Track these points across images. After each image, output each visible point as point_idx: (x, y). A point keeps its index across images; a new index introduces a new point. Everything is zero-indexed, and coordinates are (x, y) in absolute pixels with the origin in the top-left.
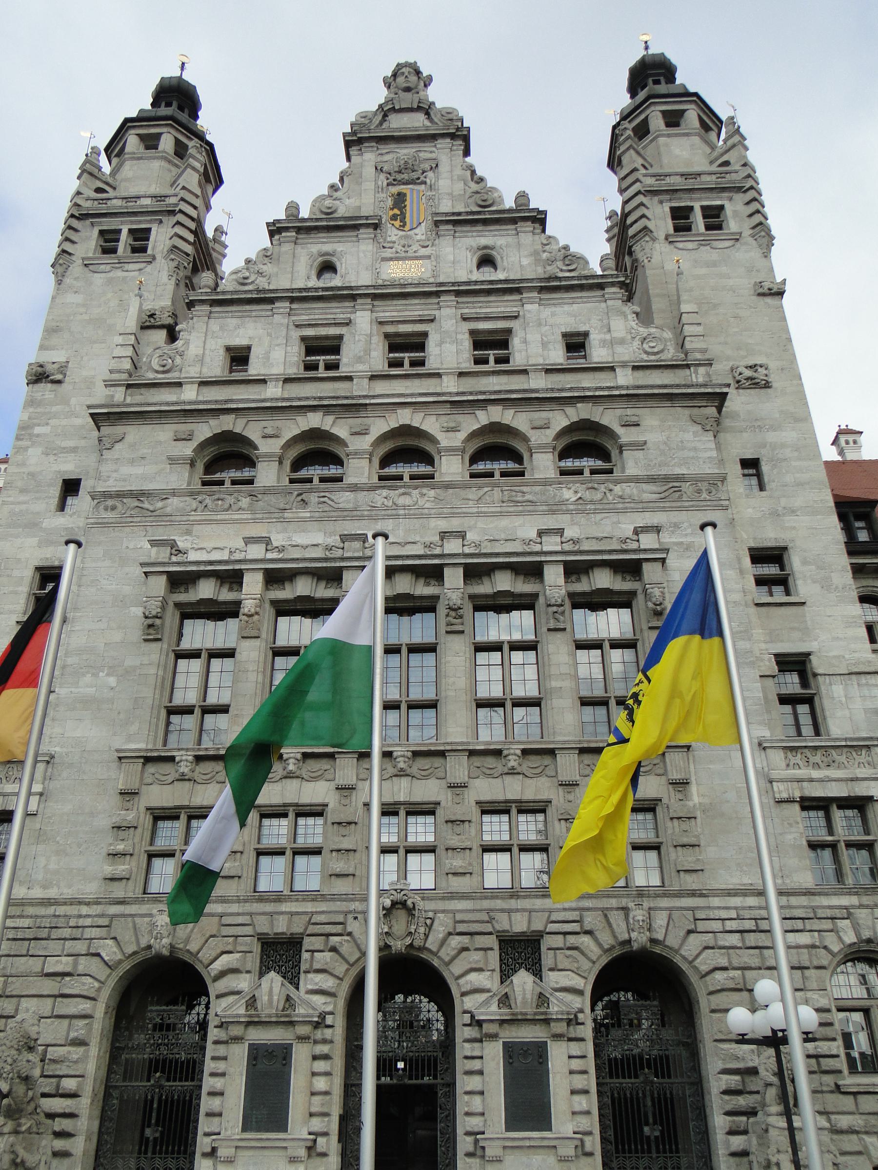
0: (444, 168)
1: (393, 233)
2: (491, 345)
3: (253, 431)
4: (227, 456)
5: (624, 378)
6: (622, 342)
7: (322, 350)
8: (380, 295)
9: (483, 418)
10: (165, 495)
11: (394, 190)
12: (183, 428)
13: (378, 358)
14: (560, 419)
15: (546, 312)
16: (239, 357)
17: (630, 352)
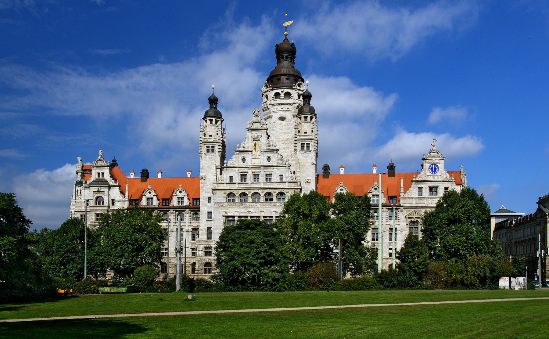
0: (263, 137)
1: (254, 152)
2: (269, 175)
3: (235, 192)
4: (230, 195)
5: (287, 185)
6: (287, 177)
7: (244, 176)
9: (267, 191)
10: (224, 203)
11: (255, 142)
12: (225, 191)
13: (252, 181)
14: (278, 191)
15: (277, 171)
16: (231, 177)
17: (289, 179)
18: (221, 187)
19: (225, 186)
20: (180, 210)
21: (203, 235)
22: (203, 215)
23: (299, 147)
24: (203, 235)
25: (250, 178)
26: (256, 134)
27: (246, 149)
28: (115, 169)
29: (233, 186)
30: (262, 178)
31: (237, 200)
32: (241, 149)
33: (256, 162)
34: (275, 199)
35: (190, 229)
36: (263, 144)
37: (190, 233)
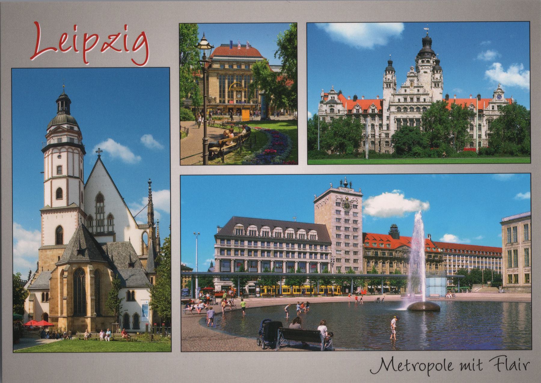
2: (418, 99)
7: (405, 99)
8: (410, 95)
16: (399, 100)
18: (394, 104)
19: (396, 104)
20: (373, 116)
21: (385, 128)
22: (385, 118)
23: (433, 85)
24: (385, 128)
25: (409, 100)
26: (412, 78)
27: (407, 85)
28: (341, 95)
29: (400, 104)
30: (415, 100)
31: (402, 110)
32: (404, 85)
33: (412, 92)
34: (422, 110)
35: (378, 124)
36: (416, 83)
37: (378, 127)
